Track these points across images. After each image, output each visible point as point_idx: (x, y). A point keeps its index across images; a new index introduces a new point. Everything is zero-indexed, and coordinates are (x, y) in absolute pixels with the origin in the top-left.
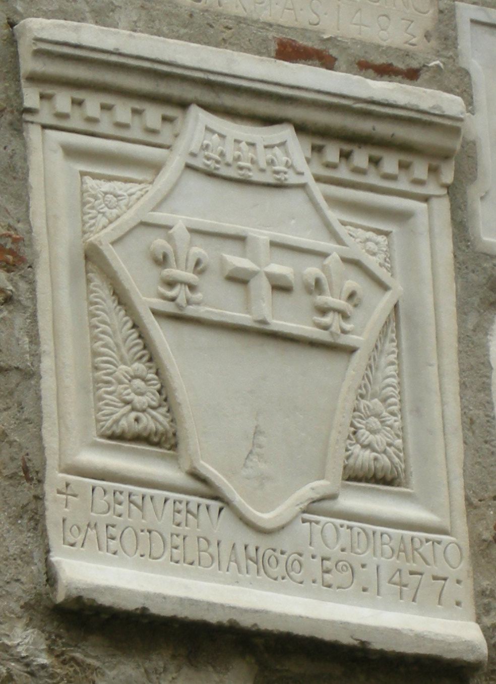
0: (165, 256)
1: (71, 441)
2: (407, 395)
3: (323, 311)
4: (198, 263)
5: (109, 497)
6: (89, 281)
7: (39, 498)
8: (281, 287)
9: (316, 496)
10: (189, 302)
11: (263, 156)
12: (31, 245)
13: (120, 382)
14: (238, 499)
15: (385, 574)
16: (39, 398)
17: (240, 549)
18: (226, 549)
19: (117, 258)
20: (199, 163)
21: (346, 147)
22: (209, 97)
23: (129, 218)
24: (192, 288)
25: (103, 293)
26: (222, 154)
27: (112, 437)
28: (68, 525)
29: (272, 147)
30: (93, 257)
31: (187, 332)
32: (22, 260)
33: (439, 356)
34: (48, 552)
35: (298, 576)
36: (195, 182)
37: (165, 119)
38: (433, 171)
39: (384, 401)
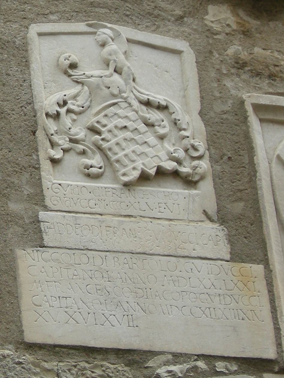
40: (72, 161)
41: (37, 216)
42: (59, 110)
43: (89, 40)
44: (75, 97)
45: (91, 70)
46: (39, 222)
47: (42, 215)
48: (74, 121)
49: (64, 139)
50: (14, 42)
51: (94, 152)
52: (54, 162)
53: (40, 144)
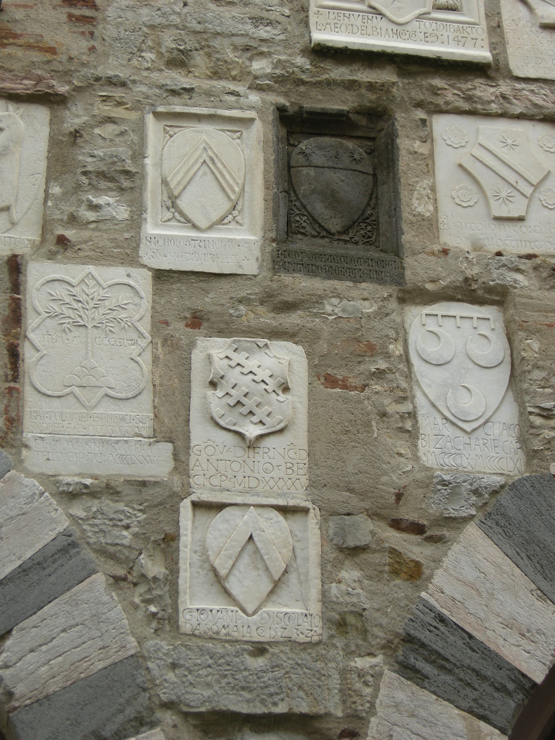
7: (307, 16)
9: (421, 13)
14: (388, 14)
17: (390, 31)
18: (384, 30)
35: (414, 39)
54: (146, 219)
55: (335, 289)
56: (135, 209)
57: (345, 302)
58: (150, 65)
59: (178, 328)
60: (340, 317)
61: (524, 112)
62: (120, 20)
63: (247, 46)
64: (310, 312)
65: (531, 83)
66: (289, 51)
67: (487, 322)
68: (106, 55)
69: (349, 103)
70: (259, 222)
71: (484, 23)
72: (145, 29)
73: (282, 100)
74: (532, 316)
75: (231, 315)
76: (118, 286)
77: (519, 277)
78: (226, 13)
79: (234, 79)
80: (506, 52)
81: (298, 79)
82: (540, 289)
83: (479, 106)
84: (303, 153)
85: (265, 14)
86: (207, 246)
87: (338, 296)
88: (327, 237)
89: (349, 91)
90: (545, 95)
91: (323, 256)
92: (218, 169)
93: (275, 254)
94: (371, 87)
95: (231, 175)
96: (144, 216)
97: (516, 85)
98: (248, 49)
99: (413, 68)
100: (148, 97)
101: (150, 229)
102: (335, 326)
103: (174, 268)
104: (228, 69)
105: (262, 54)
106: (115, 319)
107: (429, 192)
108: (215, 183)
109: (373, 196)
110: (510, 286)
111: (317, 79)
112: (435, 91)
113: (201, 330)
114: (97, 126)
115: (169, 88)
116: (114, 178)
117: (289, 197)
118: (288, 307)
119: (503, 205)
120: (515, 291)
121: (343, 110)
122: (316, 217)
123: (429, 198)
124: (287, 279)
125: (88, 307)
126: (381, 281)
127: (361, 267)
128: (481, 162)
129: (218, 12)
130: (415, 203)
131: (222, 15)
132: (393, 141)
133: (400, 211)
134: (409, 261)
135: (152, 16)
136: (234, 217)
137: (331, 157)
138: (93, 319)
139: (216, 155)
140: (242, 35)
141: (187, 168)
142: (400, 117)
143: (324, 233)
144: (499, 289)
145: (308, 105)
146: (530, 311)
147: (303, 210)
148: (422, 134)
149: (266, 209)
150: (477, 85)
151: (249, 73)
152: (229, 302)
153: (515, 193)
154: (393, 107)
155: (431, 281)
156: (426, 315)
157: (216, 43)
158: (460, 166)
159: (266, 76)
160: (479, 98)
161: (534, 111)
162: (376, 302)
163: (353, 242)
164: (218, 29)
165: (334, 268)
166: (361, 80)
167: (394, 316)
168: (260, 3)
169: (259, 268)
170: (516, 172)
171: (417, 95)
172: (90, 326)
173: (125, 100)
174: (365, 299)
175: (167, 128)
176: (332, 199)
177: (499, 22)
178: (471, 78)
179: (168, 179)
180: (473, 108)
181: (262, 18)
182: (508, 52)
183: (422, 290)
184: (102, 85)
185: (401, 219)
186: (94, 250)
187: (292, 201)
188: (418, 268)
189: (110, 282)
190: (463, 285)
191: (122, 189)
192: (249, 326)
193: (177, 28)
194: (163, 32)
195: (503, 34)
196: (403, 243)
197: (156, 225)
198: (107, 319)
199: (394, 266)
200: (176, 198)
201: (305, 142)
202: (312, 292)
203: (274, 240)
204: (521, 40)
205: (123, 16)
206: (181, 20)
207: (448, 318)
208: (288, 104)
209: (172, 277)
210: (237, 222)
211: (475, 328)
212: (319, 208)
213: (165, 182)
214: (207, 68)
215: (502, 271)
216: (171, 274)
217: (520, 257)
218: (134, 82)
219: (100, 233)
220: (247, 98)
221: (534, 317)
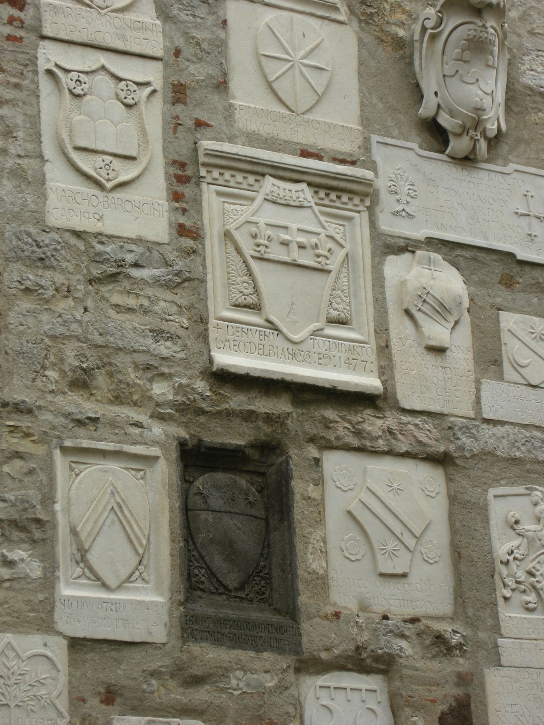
0: (256, 235)
1: (219, 307)
2: (351, 289)
3: (318, 256)
4: (269, 237)
5: (234, 329)
6: (226, 244)
7: (206, 330)
8: (302, 247)
10: (265, 253)
11: (295, 195)
12: (203, 230)
13: (238, 284)
15: (343, 360)
16: (206, 290)
17: (286, 350)
18: (280, 349)
19: (237, 235)
20: (269, 198)
21: (328, 192)
22: (273, 172)
23: (242, 219)
24: (267, 247)
25: (232, 249)
26: (278, 194)
27: (235, 306)
28: (218, 340)
29: (298, 191)
30: (227, 235)
31: (264, 264)
32: (200, 236)
33: (364, 274)
34: (210, 351)
35: (308, 361)
36: (268, 205)
37: (256, 180)
38: (362, 201)
39: (342, 291)
40: (518, 598)
41: (496, 643)
42: (509, 558)
43: (526, 499)
44: (518, 548)
45: (528, 526)
46: (498, 647)
47: (500, 641)
48: (518, 566)
49: (512, 581)
50: (479, 504)
51: (531, 591)
52: (506, 599)
53: (497, 585)
54: (59, 578)
55: (240, 660)
56: (47, 565)
57: (249, 675)
58: (54, 388)
59: (94, 703)
60: (244, 693)
61: (409, 450)
62: (21, 328)
63: (148, 364)
64: (217, 686)
65: (416, 415)
66: (189, 373)
67: (374, 694)
68: (11, 373)
69: (246, 437)
70: (167, 582)
71: (373, 341)
72: (47, 340)
73: (183, 433)
74: (417, 690)
75: (144, 691)
76: (36, 657)
77: (403, 643)
78: (127, 322)
79: (135, 404)
80: (394, 379)
81: (199, 408)
82: (423, 658)
83: (368, 443)
84: (201, 494)
85: (165, 326)
86: (118, 610)
87: (242, 669)
88: (224, 594)
89: (247, 422)
90: (429, 430)
91: (227, 622)
92: (125, 517)
93: (183, 620)
94: (268, 418)
95: (138, 525)
96: (57, 573)
97: (403, 418)
98: (148, 368)
99: (307, 396)
100: (54, 428)
101: (66, 591)
102: (240, 702)
103: (89, 635)
104: (130, 393)
105: (163, 375)
106: (35, 696)
107: (322, 544)
108: (122, 535)
109: (266, 544)
110: (397, 655)
111: (217, 408)
112: (327, 424)
113: (115, 707)
114: (5, 463)
115: (75, 417)
116: (25, 528)
117: (188, 546)
118: (196, 681)
119: (389, 560)
120: (401, 660)
121: (241, 445)
122: (214, 570)
123: (322, 552)
124: (196, 648)
125: (9, 683)
126: (280, 651)
127: (262, 634)
128: (369, 509)
129: (119, 322)
130: (309, 561)
131: (123, 325)
132: (288, 483)
133: (296, 568)
134: (305, 626)
135: (53, 324)
136: (141, 574)
137: (228, 500)
138: (15, 697)
139: (123, 501)
140: (144, 351)
141: (96, 516)
142: (293, 452)
143: (222, 590)
144: (386, 658)
145: (208, 439)
146: (415, 685)
147: (201, 562)
148: (315, 476)
149: (172, 565)
150: (366, 417)
151: (150, 398)
152: (141, 676)
153: (400, 547)
154: (287, 441)
155: (325, 650)
156: (320, 687)
157: (119, 360)
158: (349, 513)
159: (168, 404)
160: (369, 433)
161: (418, 449)
162: (276, 675)
163: (248, 600)
164: (120, 344)
165: (237, 635)
166: (258, 410)
167: (293, 690)
168: (160, 312)
169: (167, 635)
170: (401, 521)
171: (312, 429)
172: (12, 705)
173: (32, 431)
174: (267, 672)
175: (74, 465)
176: (229, 549)
177: (387, 341)
178: (360, 408)
179: (78, 529)
180: (362, 444)
181: (163, 331)
182: (396, 378)
183: (316, 659)
184: (9, 412)
185: (297, 577)
186: (10, 614)
187: (189, 550)
188: (315, 635)
189: (29, 653)
190: (354, 654)
191: (34, 541)
192: (161, 704)
193: (79, 340)
194: (64, 344)
195: (391, 356)
196: (300, 605)
197: (68, 584)
198: (28, 697)
199: (291, 633)
200: (86, 551)
201: (201, 478)
202: (218, 665)
203: (181, 604)
204: (407, 364)
205: (24, 323)
206: (82, 330)
207: (339, 690)
208: (187, 437)
209: (86, 646)
210: (143, 579)
211: (364, 701)
212: (217, 561)
213: (74, 532)
214: (109, 390)
215: (390, 637)
216: (85, 642)
217: (405, 621)
218: (40, 408)
219: (14, 594)
220: (151, 431)
221: (420, 692)
